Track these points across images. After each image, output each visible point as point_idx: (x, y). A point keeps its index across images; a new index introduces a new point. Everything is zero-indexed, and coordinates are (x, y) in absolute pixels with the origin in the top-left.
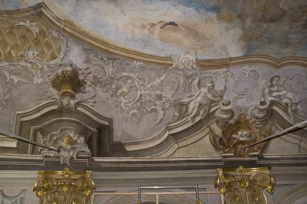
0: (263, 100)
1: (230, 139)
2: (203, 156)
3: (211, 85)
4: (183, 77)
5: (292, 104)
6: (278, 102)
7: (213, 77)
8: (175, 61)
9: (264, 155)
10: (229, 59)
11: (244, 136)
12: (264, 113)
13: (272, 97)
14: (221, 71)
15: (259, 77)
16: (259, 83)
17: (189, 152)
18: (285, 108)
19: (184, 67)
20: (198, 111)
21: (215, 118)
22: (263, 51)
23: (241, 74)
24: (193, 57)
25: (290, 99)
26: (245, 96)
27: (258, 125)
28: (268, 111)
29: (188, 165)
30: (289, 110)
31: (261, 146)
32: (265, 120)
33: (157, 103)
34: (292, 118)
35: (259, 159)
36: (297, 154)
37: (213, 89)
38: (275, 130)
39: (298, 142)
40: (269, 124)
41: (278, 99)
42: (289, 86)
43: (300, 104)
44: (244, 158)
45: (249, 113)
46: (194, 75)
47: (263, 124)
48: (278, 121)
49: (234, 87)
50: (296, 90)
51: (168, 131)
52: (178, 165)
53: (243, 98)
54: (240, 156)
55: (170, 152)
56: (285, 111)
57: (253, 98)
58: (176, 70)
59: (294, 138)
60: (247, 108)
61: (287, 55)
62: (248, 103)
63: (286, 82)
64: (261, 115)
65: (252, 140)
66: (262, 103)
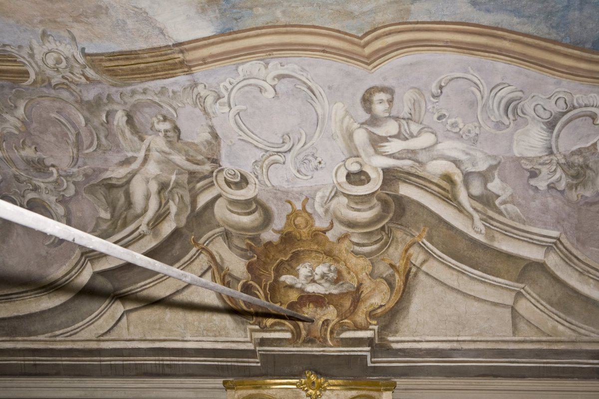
0: (355, 168)
1: (274, 290)
2: (199, 336)
3: (167, 126)
4: (77, 106)
5: (467, 176)
6: (413, 171)
7: (162, 104)
8: (27, 63)
9: (391, 339)
10: (177, 48)
11: (320, 279)
12: (371, 208)
13: (387, 156)
14: (175, 83)
15: (315, 95)
16: (324, 115)
17: (158, 326)
18: (444, 189)
19: (63, 77)
20: (163, 205)
21: (218, 226)
22: (284, 12)
23: (246, 89)
24: (68, 46)
25: (457, 162)
26: (289, 156)
27: (358, 244)
28: (385, 203)
29: (157, 362)
30: (463, 197)
31: (379, 311)
32: (383, 228)
33: (39, 182)
34: (479, 224)
35: (374, 354)
36: (504, 338)
37: (179, 138)
38: (425, 261)
39: (508, 299)
40: (397, 241)
41: (409, 162)
42: (439, 118)
43: (496, 176)
44: (325, 347)
45: (320, 210)
46: (105, 101)
47: (376, 242)
48: (428, 233)
49: (241, 130)
50: (469, 131)
51: (89, 264)
52: (129, 362)
53: (284, 163)
54: (310, 341)
55: (104, 323)
56: (450, 199)
57: (320, 163)
58: (45, 86)
59: (495, 286)
60: (306, 193)
61: (380, 18)
62: (305, 178)
63: (423, 104)
64: (365, 215)
65: (347, 293)
66: (357, 177)
